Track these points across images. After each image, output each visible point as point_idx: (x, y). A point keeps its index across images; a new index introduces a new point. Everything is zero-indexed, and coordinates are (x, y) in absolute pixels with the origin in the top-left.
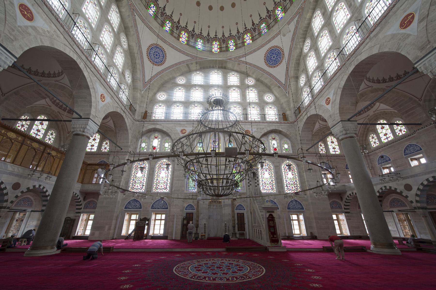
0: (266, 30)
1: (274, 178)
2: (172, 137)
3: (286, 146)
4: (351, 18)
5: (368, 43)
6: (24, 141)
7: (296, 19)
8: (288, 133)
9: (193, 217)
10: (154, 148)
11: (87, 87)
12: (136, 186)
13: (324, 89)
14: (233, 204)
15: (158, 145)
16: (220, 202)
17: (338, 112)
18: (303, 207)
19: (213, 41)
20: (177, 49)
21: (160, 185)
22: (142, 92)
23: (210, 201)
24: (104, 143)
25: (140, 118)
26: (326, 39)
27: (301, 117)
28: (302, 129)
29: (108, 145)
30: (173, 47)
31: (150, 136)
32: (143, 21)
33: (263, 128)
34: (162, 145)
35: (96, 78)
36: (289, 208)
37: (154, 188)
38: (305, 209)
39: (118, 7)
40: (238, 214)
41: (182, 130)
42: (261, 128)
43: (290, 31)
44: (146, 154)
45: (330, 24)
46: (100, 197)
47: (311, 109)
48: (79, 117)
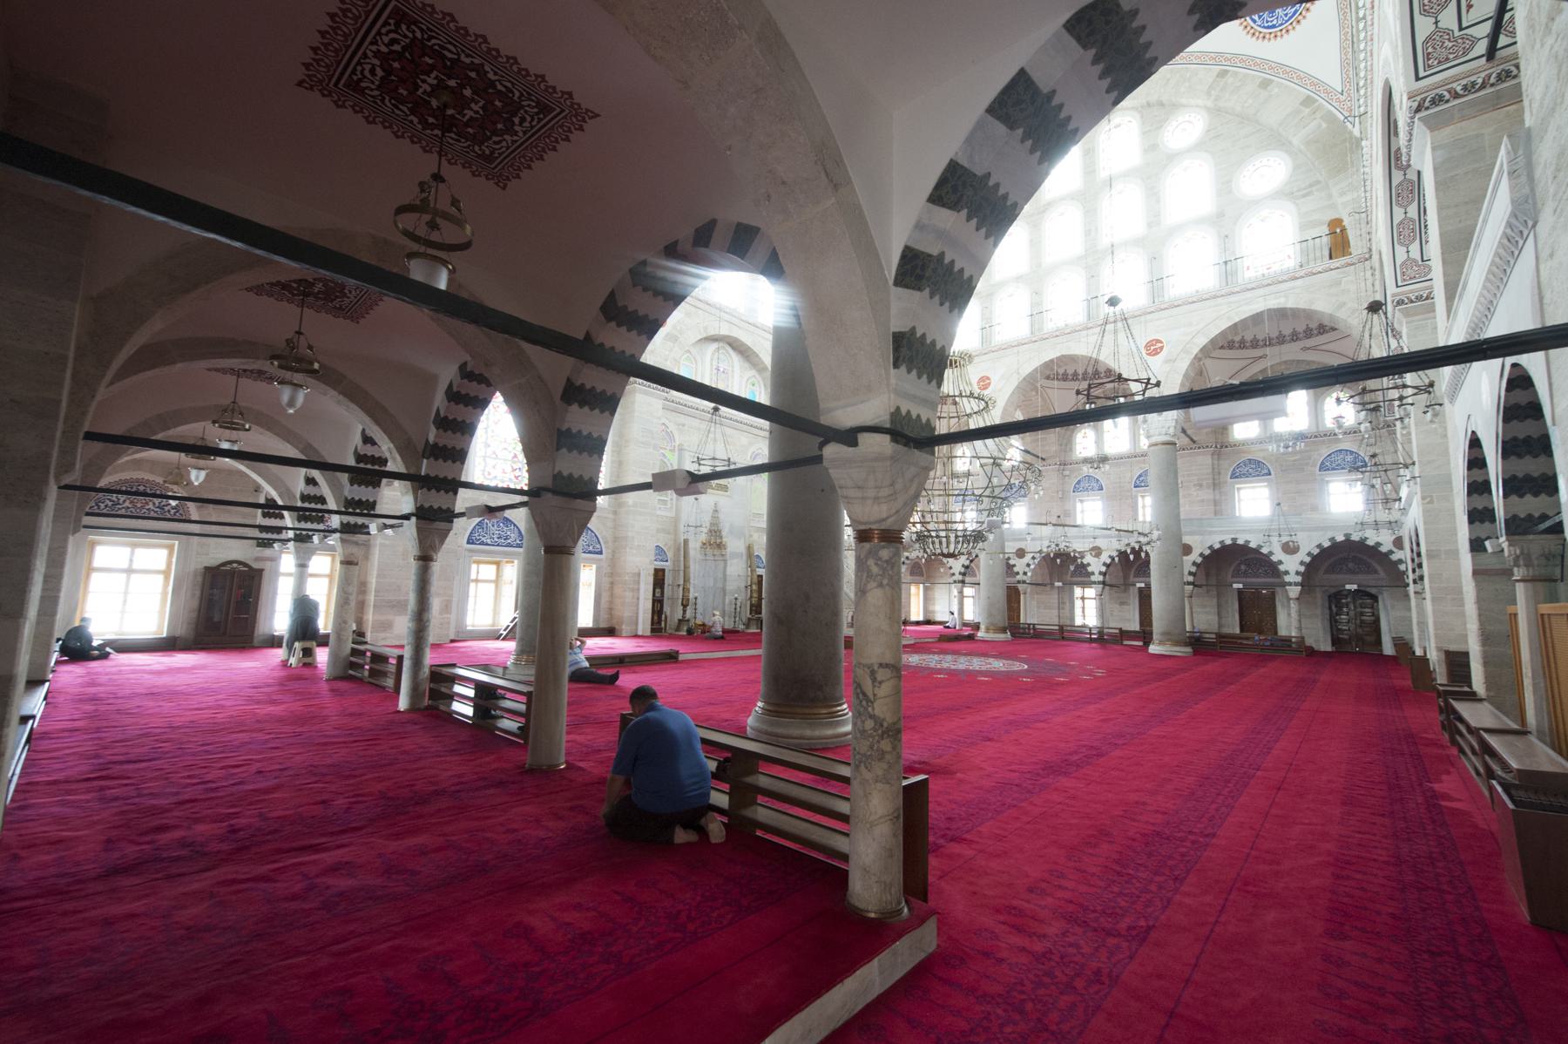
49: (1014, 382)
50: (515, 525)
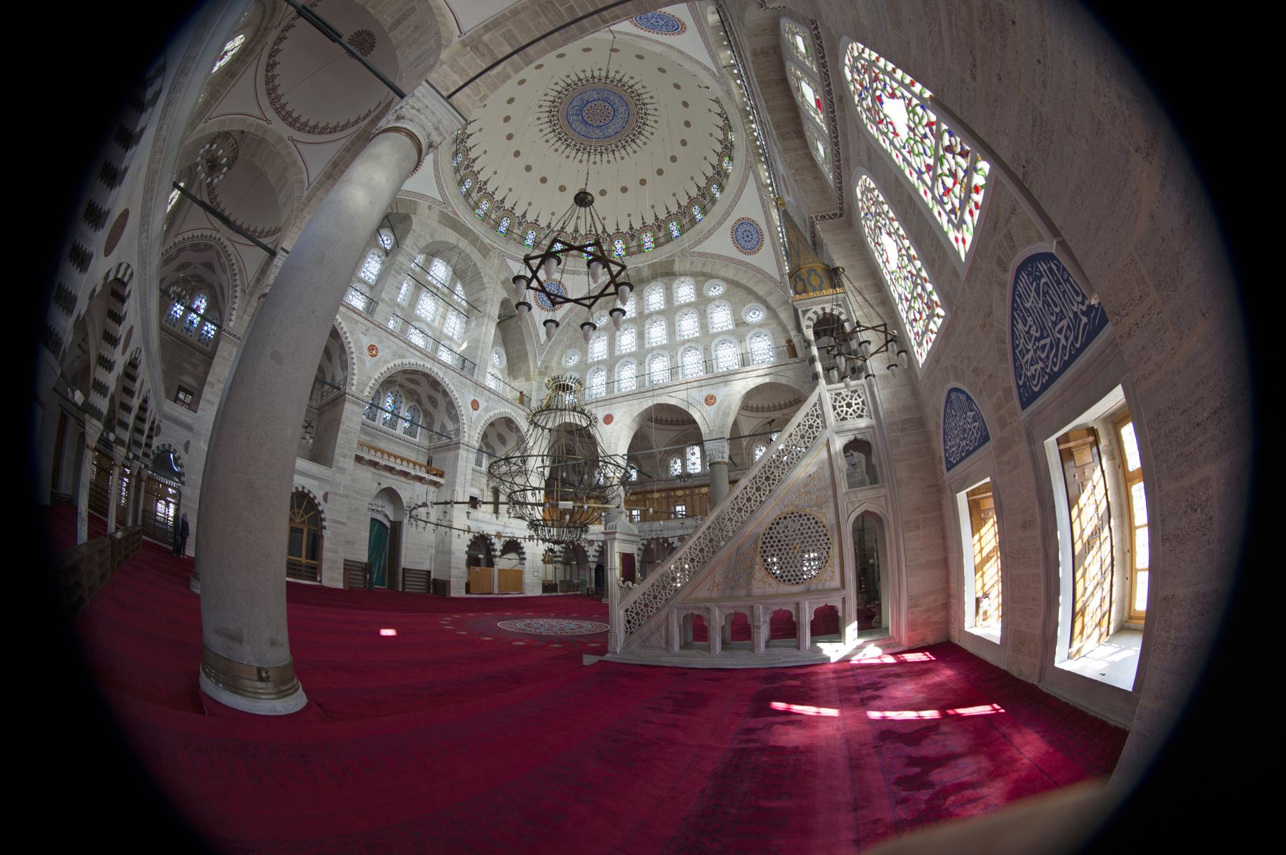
6: (692, 492)
32: (700, 242)
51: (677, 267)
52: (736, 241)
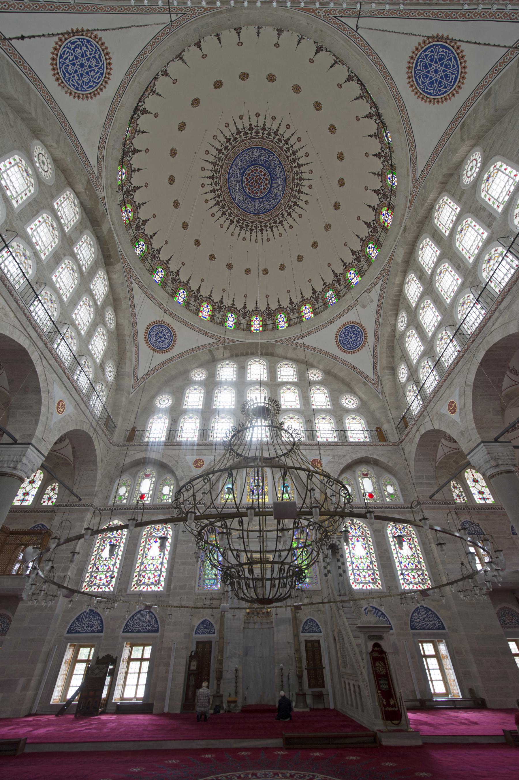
0: (334, 300)
1: (374, 555)
2: (177, 474)
3: (390, 489)
4: (463, 284)
5: (498, 318)
7: (380, 284)
8: (390, 464)
9: (211, 652)
10: (142, 497)
11: (38, 390)
12: (98, 578)
13: (441, 386)
14: (295, 619)
15: (150, 490)
16: (268, 612)
17: (474, 425)
18: (442, 624)
19: (252, 316)
20: (194, 328)
21: (146, 577)
22: (131, 395)
23: (248, 610)
24: (50, 488)
25: (121, 440)
26: (431, 312)
27: (410, 435)
28: (416, 456)
29: (56, 491)
30: (188, 325)
31: (136, 473)
33: (344, 456)
34: (156, 490)
35: (55, 374)
36: (413, 628)
37: (133, 583)
38: (449, 628)
39: (108, 273)
40: (306, 642)
41: (196, 461)
42: (340, 456)
43: (372, 301)
44: (125, 509)
45: (432, 291)
46: (21, 605)
47: (426, 420)
48: (13, 442)
49: (469, 392)
50: (100, 616)
51: (118, 266)
52: (152, 327)
